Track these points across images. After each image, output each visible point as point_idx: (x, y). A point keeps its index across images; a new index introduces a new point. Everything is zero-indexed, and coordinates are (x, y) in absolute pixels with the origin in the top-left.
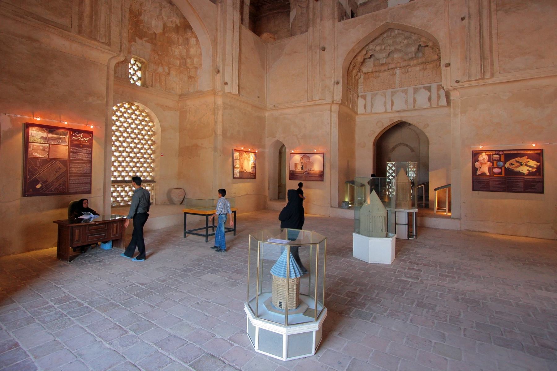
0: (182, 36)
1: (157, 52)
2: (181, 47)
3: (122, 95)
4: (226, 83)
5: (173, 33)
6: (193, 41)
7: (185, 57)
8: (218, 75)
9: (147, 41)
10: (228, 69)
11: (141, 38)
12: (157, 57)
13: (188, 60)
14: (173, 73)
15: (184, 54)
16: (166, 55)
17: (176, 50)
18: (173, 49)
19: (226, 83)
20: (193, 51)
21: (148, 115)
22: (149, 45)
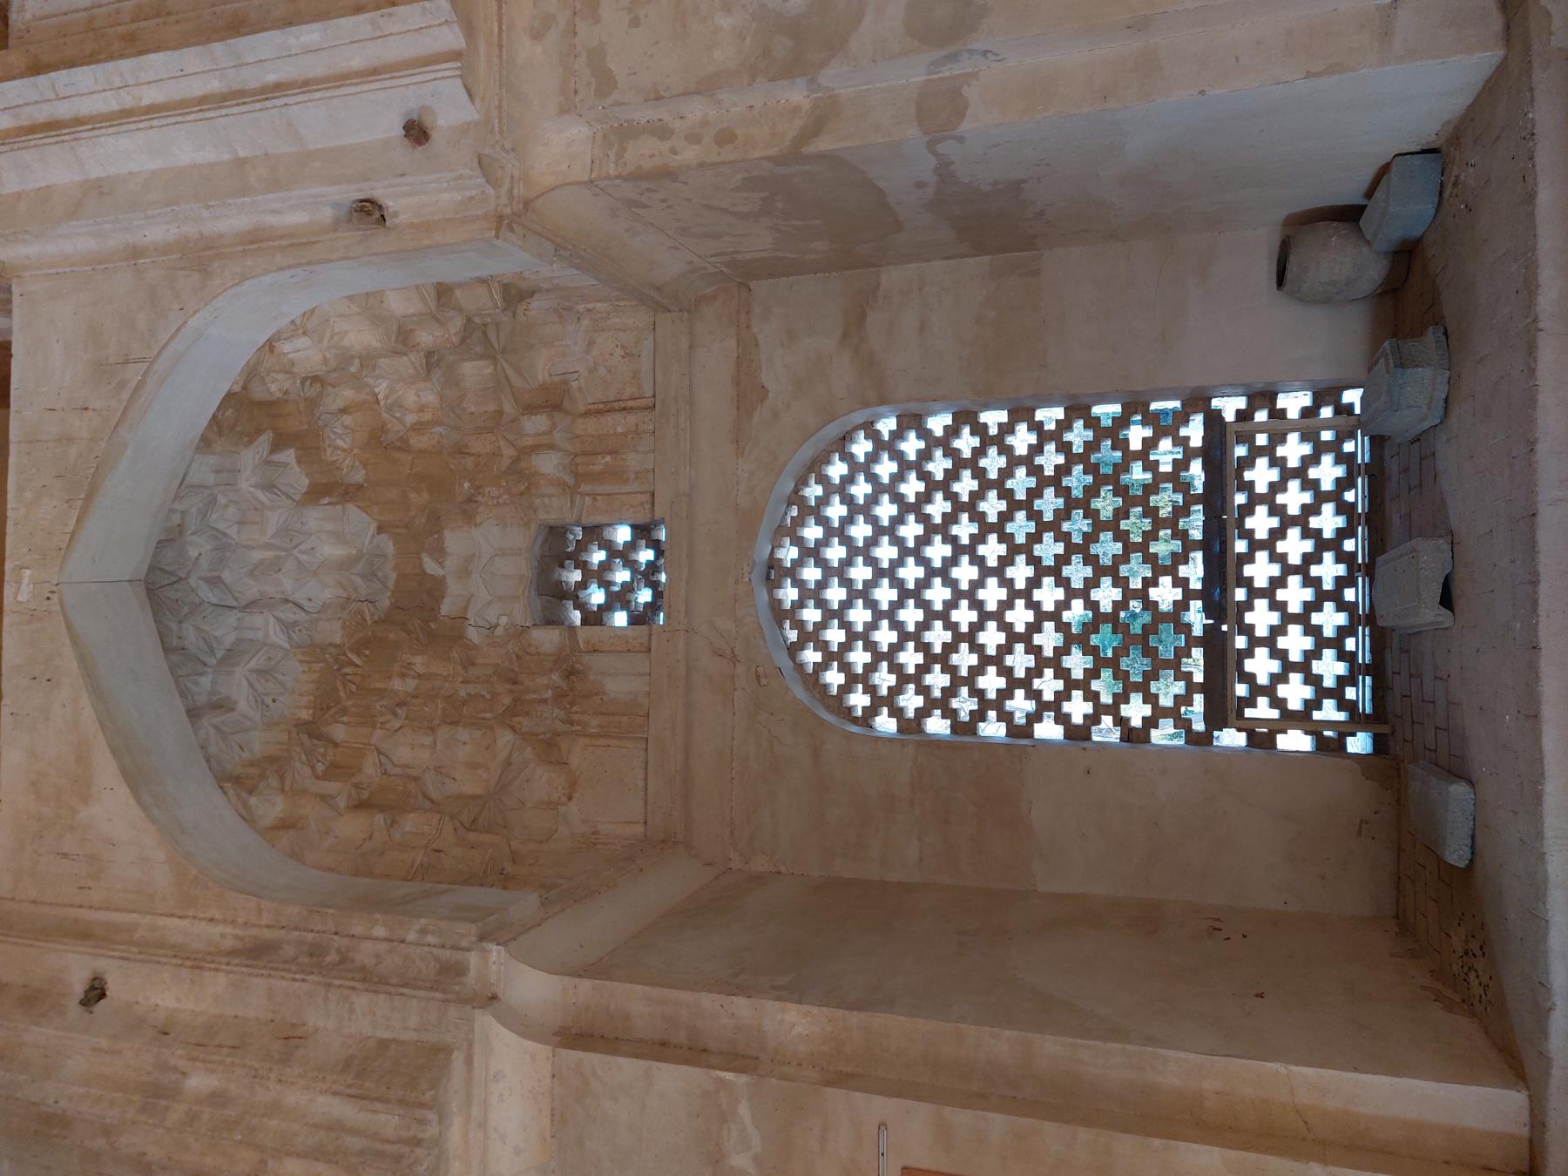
0: (312, 403)
1: (470, 499)
2: (382, 388)
3: (734, 660)
4: (416, 132)
5: (329, 455)
6: (304, 353)
7: (416, 358)
8: (390, 204)
9: (440, 553)
10: (319, 123)
11: (436, 589)
12: (494, 491)
13: (425, 338)
14: (541, 368)
15: (407, 364)
16: (460, 451)
17: (410, 398)
18: (411, 419)
19: (416, 132)
20: (360, 336)
21: (816, 467)
22: (455, 541)
